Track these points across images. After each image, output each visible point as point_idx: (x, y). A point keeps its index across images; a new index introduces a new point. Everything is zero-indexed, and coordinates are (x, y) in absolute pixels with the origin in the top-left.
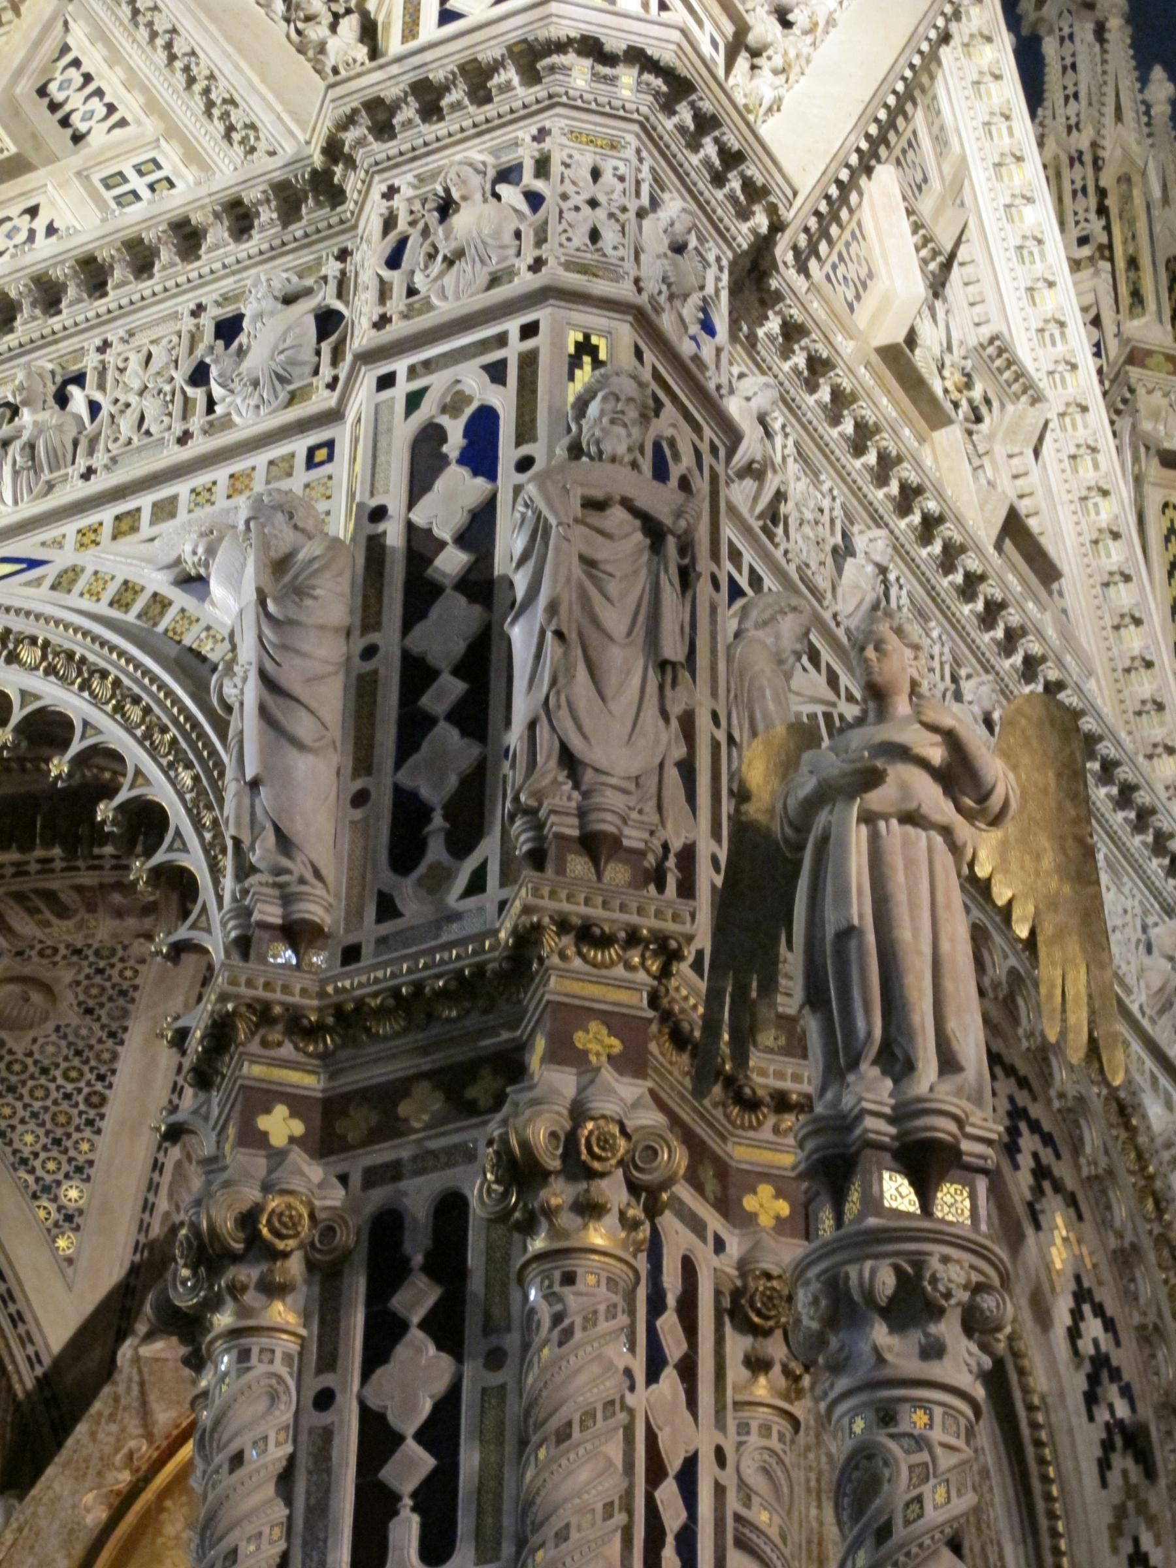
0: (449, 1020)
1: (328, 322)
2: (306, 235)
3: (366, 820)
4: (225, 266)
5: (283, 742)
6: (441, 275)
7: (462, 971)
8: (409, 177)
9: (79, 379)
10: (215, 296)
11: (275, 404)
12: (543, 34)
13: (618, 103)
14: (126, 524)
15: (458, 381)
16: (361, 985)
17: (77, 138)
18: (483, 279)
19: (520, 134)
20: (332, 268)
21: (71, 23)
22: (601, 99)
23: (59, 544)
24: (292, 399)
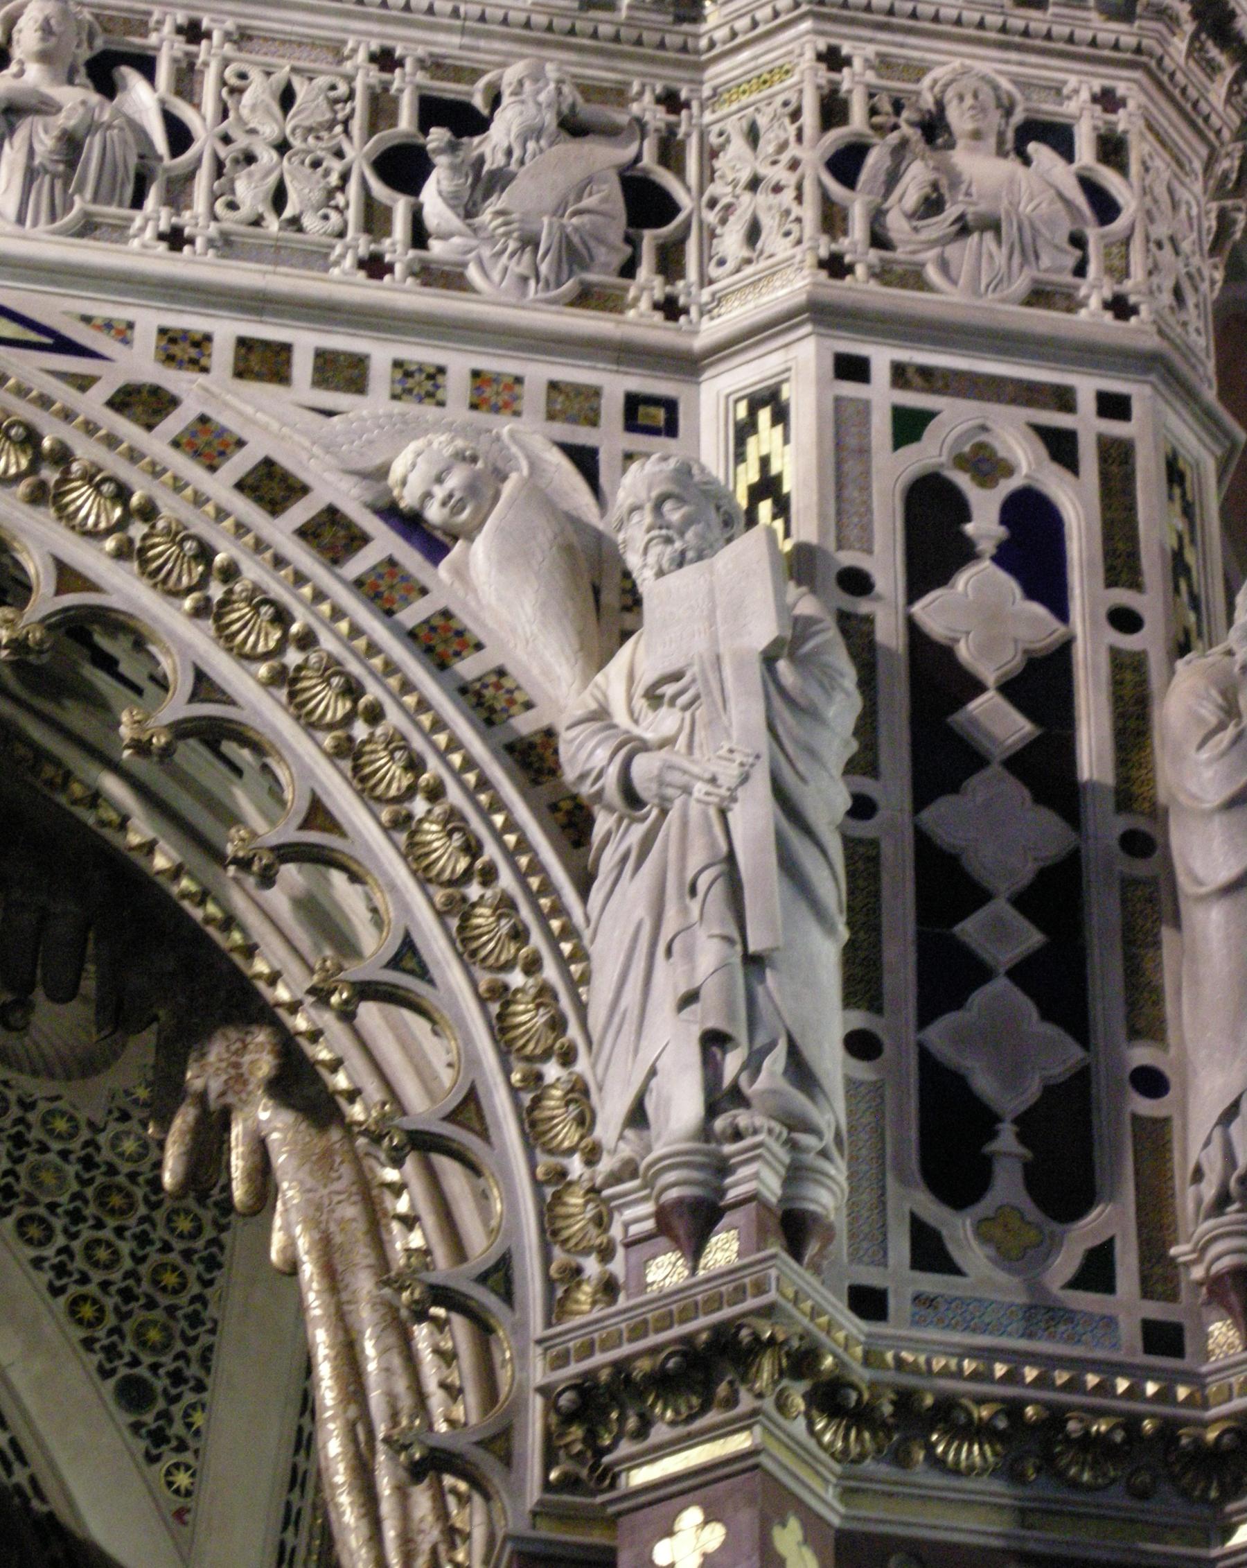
0: (1075, 1485)
2: (616, 38)
3: (877, 1088)
5: (803, 909)
6: (943, 241)
7: (1140, 1417)
8: (870, 50)
9: (146, 66)
10: (421, 51)
11: (554, 293)
13: (1204, 106)
14: (263, 362)
15: (984, 428)
16: (945, 1373)
18: (1021, 284)
22: (1193, 93)
23: (124, 332)
24: (585, 298)
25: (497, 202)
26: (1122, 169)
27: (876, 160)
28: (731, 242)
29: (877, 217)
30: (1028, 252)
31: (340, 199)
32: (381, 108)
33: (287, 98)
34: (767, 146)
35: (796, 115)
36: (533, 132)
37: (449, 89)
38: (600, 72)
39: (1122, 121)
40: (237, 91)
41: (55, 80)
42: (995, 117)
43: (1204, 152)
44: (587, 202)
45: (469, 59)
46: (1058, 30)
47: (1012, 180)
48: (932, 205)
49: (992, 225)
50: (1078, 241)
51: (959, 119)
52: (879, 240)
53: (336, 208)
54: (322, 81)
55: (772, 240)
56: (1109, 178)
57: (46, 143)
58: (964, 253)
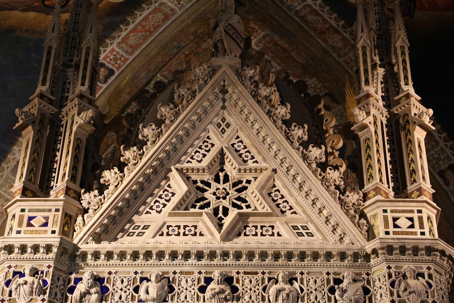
1: (366, 291)
2: (359, 266)
4: (337, 265)
8: (394, 265)
9: (296, 279)
10: (333, 271)
12: (435, 247)
13: (443, 265)
17: (283, 212)
19: (423, 266)
20: (365, 276)
21: (276, 179)
22: (441, 264)
25: (345, 295)
26: (432, 279)
27: (397, 283)
28: (378, 297)
29: (398, 292)
30: (419, 295)
31: (324, 297)
32: (328, 281)
33: (315, 282)
34: (382, 282)
35: (385, 277)
36: (350, 283)
37: (337, 277)
38: (357, 271)
39: (432, 271)
40: (309, 282)
41: (285, 284)
42: (413, 273)
43: (444, 271)
44: (358, 293)
45: (339, 271)
46: (421, 259)
47: (416, 284)
48: (405, 290)
49: (414, 292)
50: (427, 292)
51: (408, 274)
52: (399, 296)
53: (324, 299)
54: (320, 278)
55: (383, 297)
56: (430, 281)
57: (285, 296)
58: (411, 297)
